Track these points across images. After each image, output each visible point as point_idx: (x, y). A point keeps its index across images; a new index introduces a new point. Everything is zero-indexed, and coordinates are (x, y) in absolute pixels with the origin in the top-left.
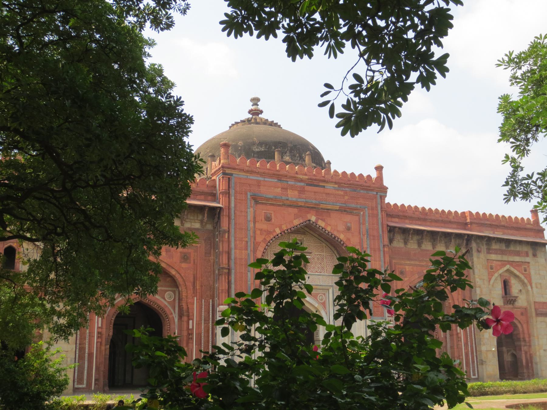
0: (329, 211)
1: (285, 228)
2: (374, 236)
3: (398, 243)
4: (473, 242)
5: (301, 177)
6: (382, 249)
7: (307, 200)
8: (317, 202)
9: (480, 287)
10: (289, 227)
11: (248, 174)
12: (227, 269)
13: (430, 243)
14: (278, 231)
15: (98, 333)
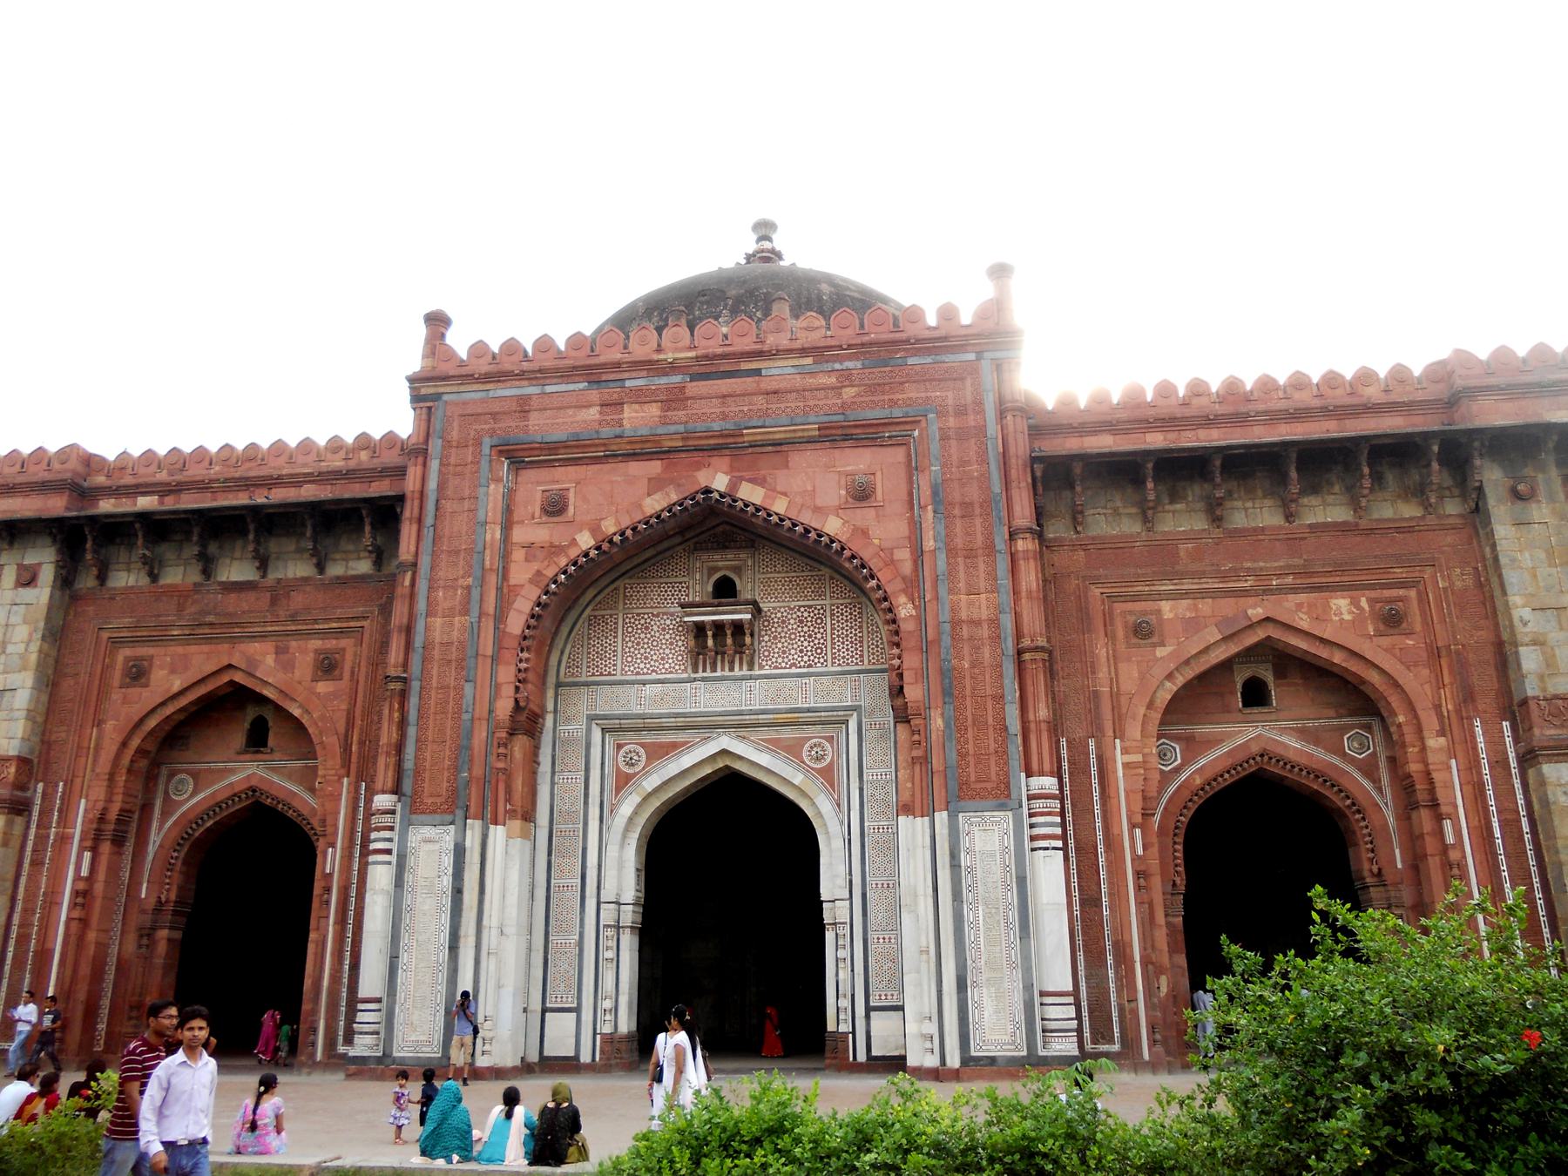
0: (784, 448)
1: (612, 530)
2: (967, 505)
3: (1112, 520)
4: (1477, 462)
5: (670, 356)
6: (1000, 543)
7: (690, 426)
8: (729, 426)
9: (1535, 643)
10: (626, 522)
11: (488, 386)
12: (398, 679)
13: (1268, 502)
14: (586, 541)
15: (76, 893)
